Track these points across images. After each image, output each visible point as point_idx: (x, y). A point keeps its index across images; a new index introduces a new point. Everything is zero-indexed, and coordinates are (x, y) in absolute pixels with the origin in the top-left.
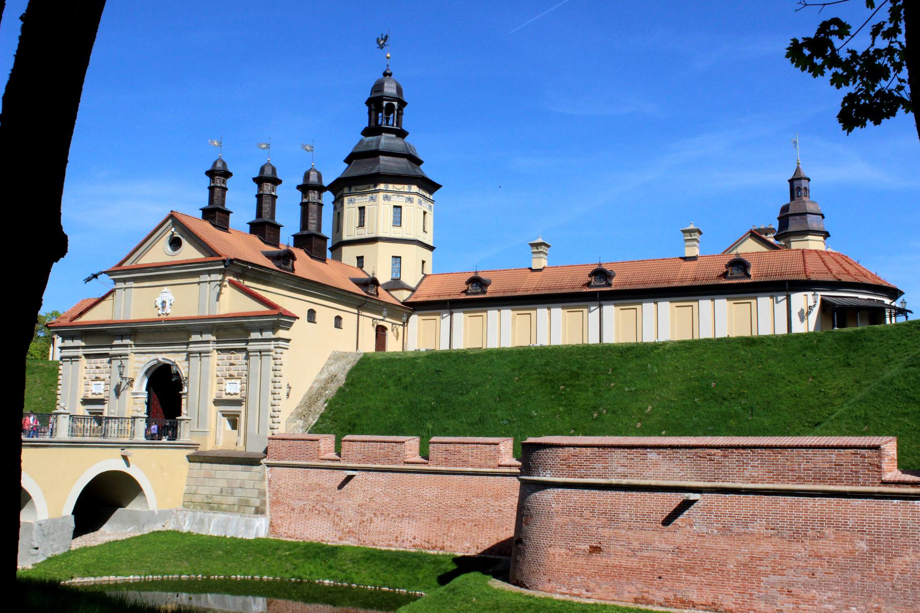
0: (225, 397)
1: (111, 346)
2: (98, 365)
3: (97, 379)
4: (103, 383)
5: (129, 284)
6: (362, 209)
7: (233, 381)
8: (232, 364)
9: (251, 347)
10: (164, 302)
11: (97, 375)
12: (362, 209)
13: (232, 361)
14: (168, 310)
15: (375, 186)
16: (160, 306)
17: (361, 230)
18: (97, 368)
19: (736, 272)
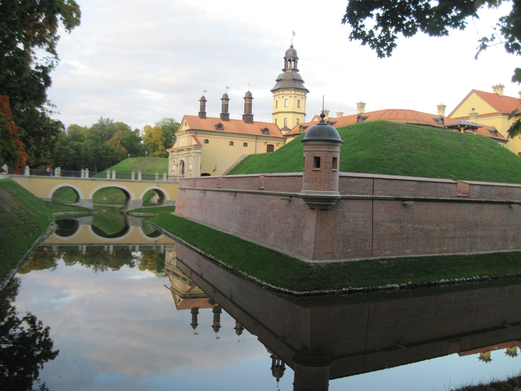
6: (299, 101)
12: (299, 101)
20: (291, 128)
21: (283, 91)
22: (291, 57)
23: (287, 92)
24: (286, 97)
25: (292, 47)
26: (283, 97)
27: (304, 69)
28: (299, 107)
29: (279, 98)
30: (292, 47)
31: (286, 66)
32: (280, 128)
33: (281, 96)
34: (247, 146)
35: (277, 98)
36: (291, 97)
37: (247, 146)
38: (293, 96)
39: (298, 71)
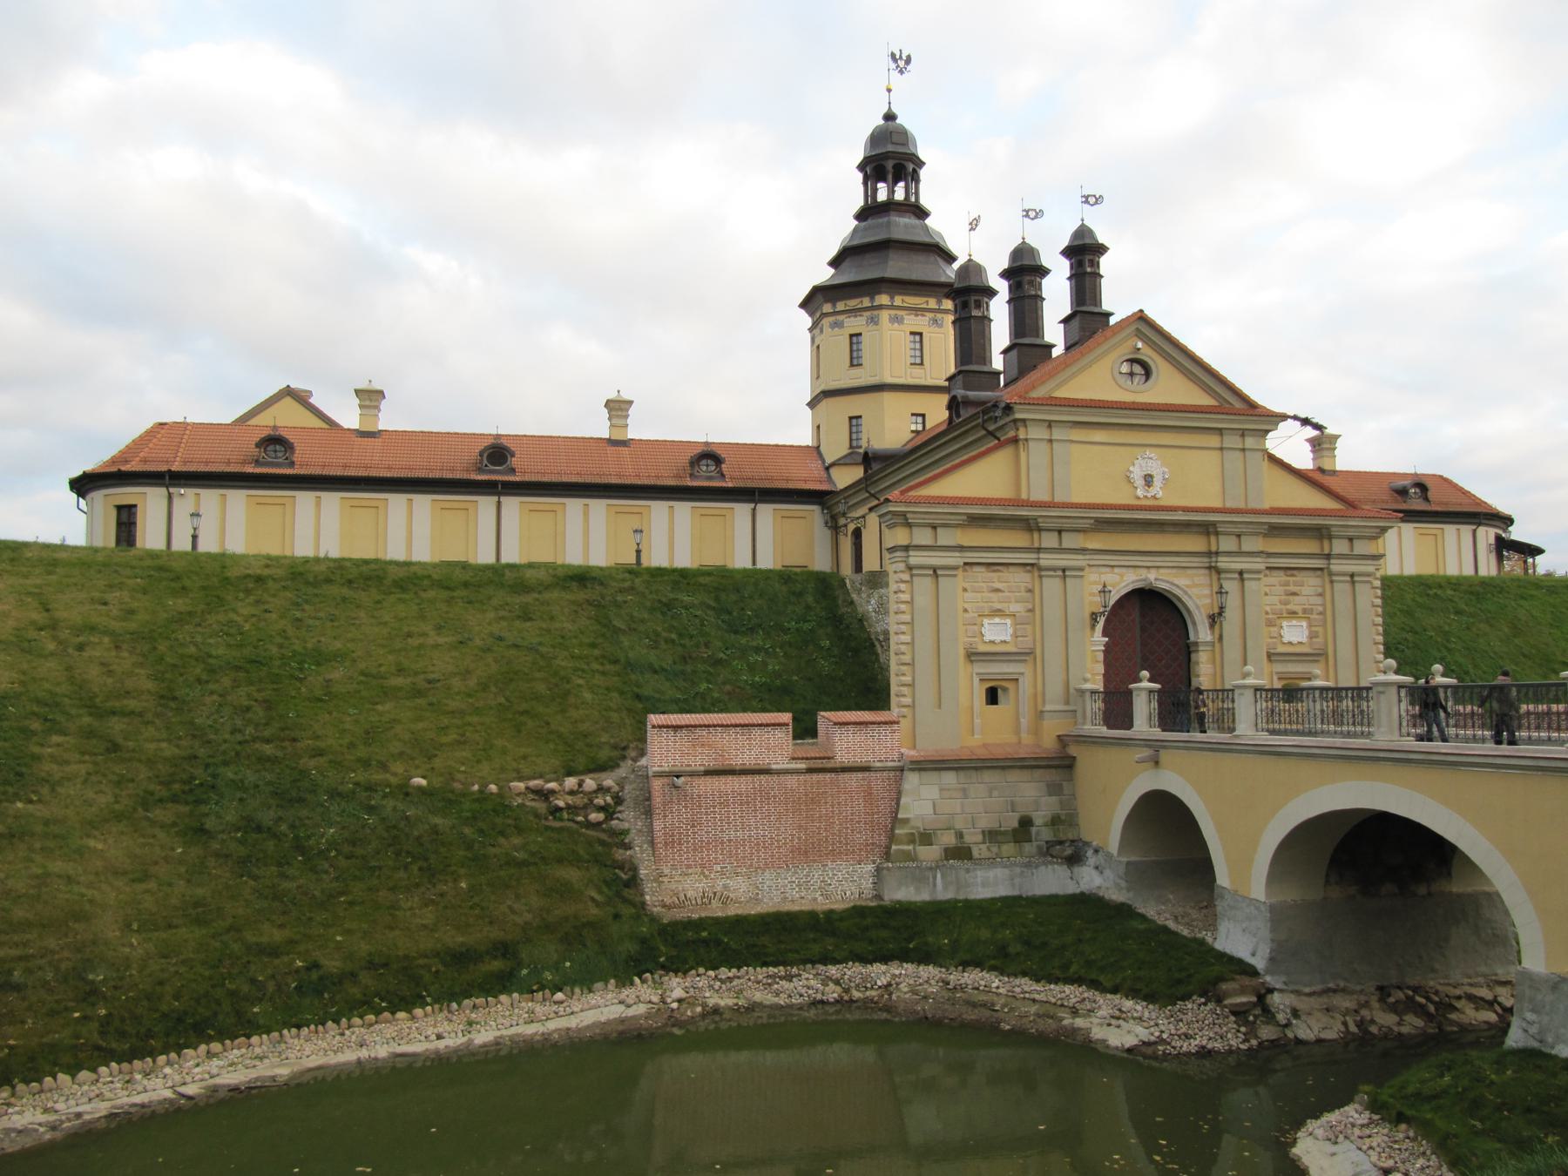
0: (1281, 649)
1: (1039, 550)
2: (997, 585)
3: (998, 613)
4: (1008, 621)
5: (1057, 434)
7: (1294, 622)
8: (1294, 594)
9: (1336, 566)
10: (1148, 480)
11: (999, 606)
13: (1292, 588)
14: (1157, 489)
15: (939, 302)
16: (1140, 482)
18: (998, 590)
19: (707, 468)
22: (890, 159)
23: (853, 303)
24: (854, 324)
25: (890, 117)
26: (836, 325)
30: (890, 117)
32: (828, 461)
36: (874, 321)
38: (885, 315)
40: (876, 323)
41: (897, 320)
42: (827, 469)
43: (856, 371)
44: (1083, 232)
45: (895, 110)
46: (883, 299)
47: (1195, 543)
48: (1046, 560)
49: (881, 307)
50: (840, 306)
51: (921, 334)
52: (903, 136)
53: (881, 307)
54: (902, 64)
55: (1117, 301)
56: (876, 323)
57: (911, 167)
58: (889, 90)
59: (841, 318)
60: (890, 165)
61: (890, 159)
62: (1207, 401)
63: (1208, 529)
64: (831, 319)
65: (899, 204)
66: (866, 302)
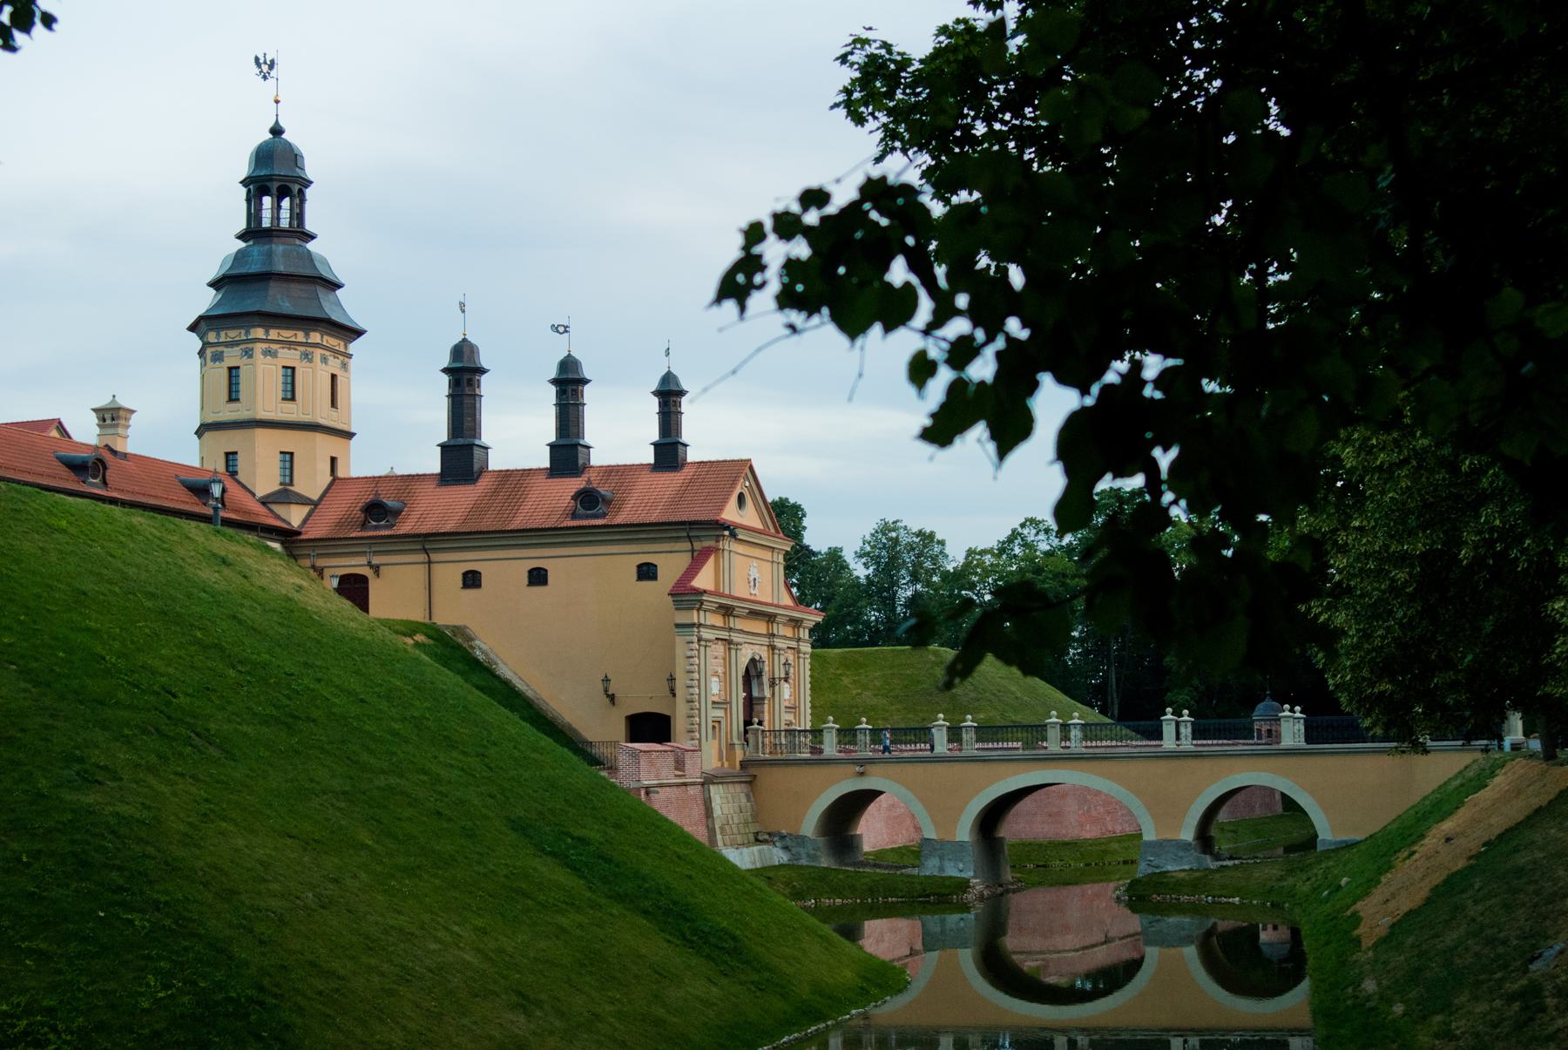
12: (334, 377)
17: (333, 413)
20: (315, 497)
21: (267, 329)
23: (287, 334)
24: (289, 357)
25: (277, 131)
26: (274, 354)
27: (334, 234)
28: (233, 397)
29: (248, 353)
30: (277, 131)
31: (254, 215)
32: (260, 493)
33: (259, 347)
34: (466, 586)
35: (232, 357)
36: (307, 357)
37: (466, 586)
38: (318, 352)
39: (312, 237)
40: (311, 361)
41: (324, 360)
42: (265, 502)
43: (289, 405)
44: (669, 378)
45: (282, 123)
46: (315, 337)
47: (760, 627)
48: (736, 637)
49: (316, 345)
50: (273, 334)
51: (334, 377)
52: (294, 157)
53: (316, 345)
54: (265, 68)
55: (705, 438)
56: (311, 361)
57: (296, 188)
58: (277, 102)
59: (274, 347)
60: (275, 186)
61: (276, 175)
62: (759, 526)
63: (770, 618)
64: (264, 346)
65: (283, 231)
66: (301, 337)
